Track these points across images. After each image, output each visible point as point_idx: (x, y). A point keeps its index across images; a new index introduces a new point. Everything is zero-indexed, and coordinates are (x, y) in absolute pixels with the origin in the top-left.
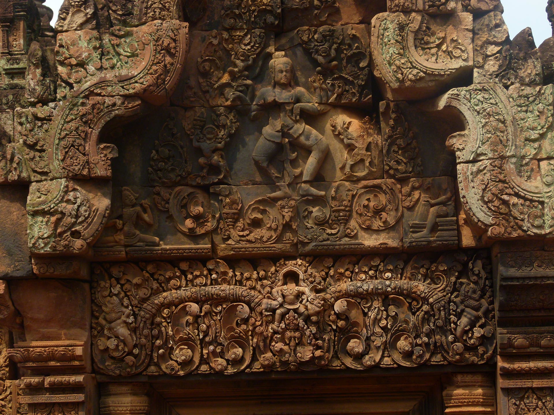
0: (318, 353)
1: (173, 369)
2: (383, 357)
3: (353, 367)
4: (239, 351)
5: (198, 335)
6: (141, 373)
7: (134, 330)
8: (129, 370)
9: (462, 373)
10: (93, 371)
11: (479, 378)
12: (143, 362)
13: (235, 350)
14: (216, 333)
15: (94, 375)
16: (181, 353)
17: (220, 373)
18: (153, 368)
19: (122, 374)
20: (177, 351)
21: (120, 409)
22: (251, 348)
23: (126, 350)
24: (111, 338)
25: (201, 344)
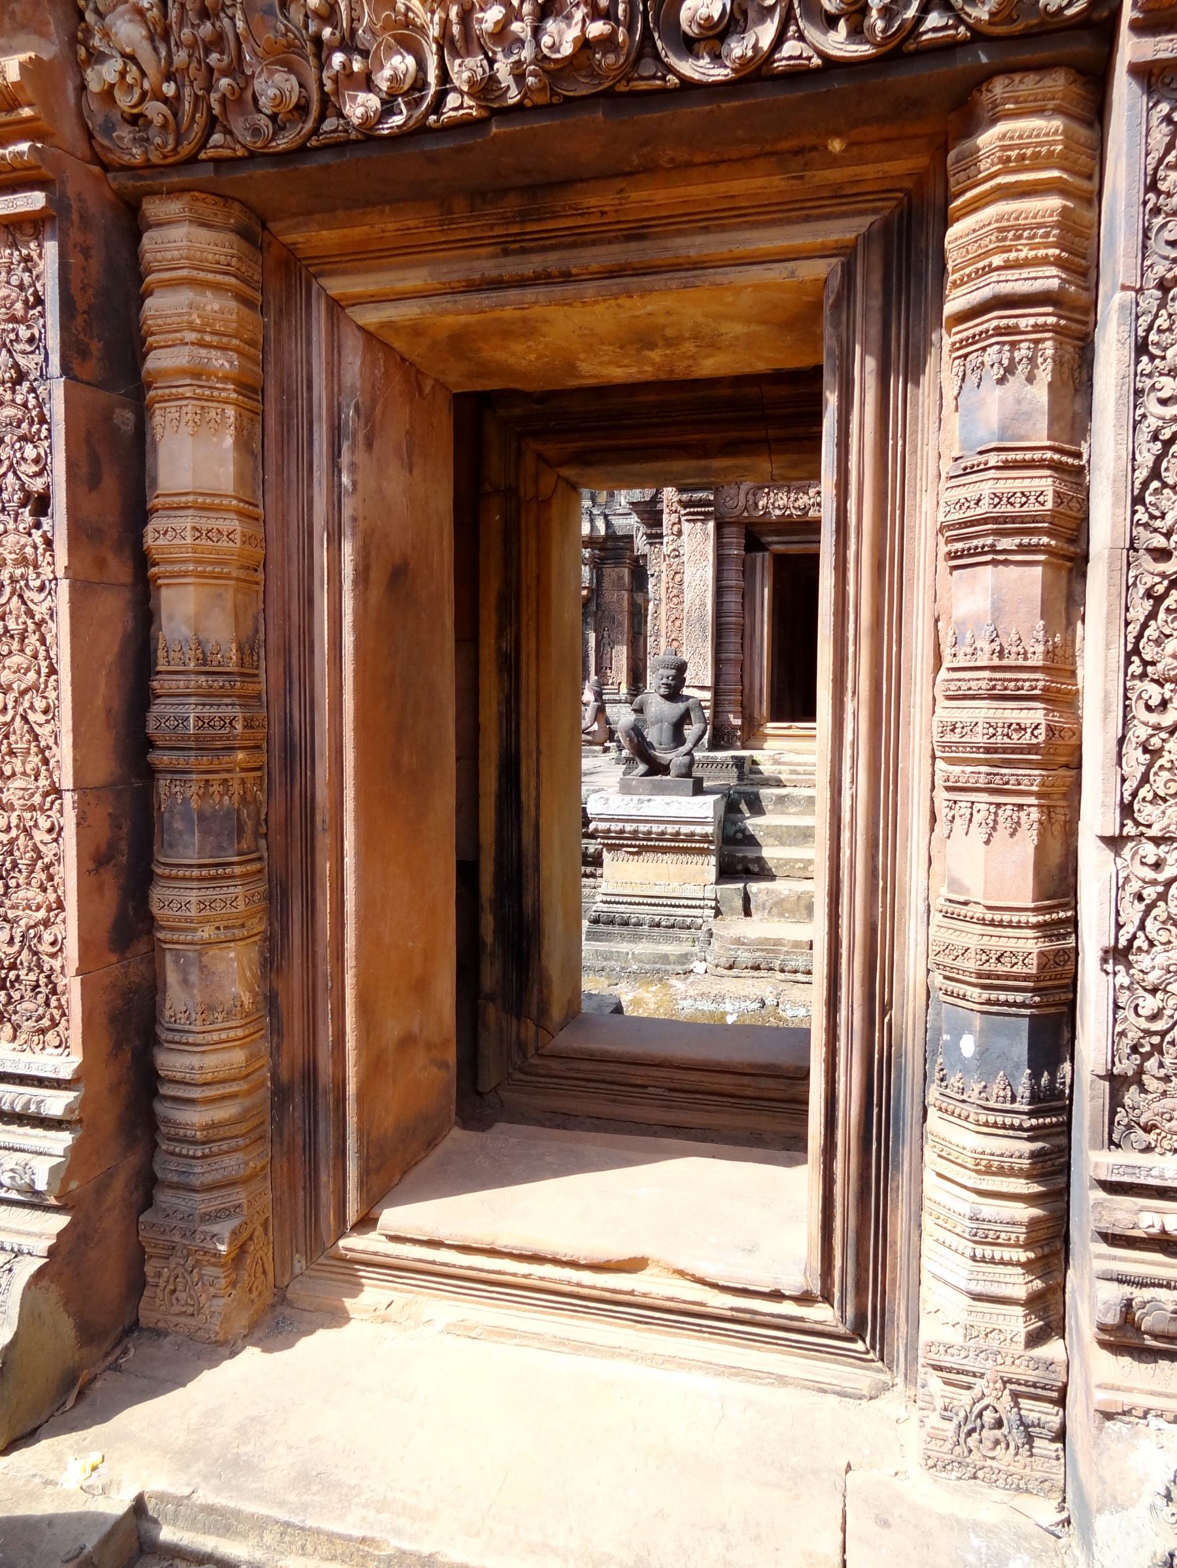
0: (597, 29)
1: (256, 131)
2: (779, 40)
3: (696, 76)
4: (404, 63)
5: (306, 27)
6: (192, 160)
7: (161, 34)
8: (158, 140)
9: (1008, 70)
10: (97, 160)
11: (1057, 83)
12: (193, 120)
13: (396, 60)
14: (352, 20)
15: (96, 169)
16: (274, 87)
17: (367, 135)
18: (217, 138)
19: (155, 158)
20: (262, 79)
21: (168, 255)
22: (434, 47)
23: (146, 86)
24: (113, 57)
25: (318, 56)
